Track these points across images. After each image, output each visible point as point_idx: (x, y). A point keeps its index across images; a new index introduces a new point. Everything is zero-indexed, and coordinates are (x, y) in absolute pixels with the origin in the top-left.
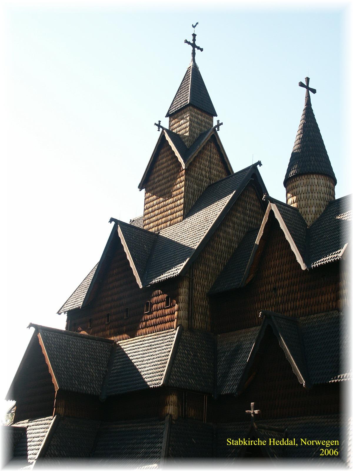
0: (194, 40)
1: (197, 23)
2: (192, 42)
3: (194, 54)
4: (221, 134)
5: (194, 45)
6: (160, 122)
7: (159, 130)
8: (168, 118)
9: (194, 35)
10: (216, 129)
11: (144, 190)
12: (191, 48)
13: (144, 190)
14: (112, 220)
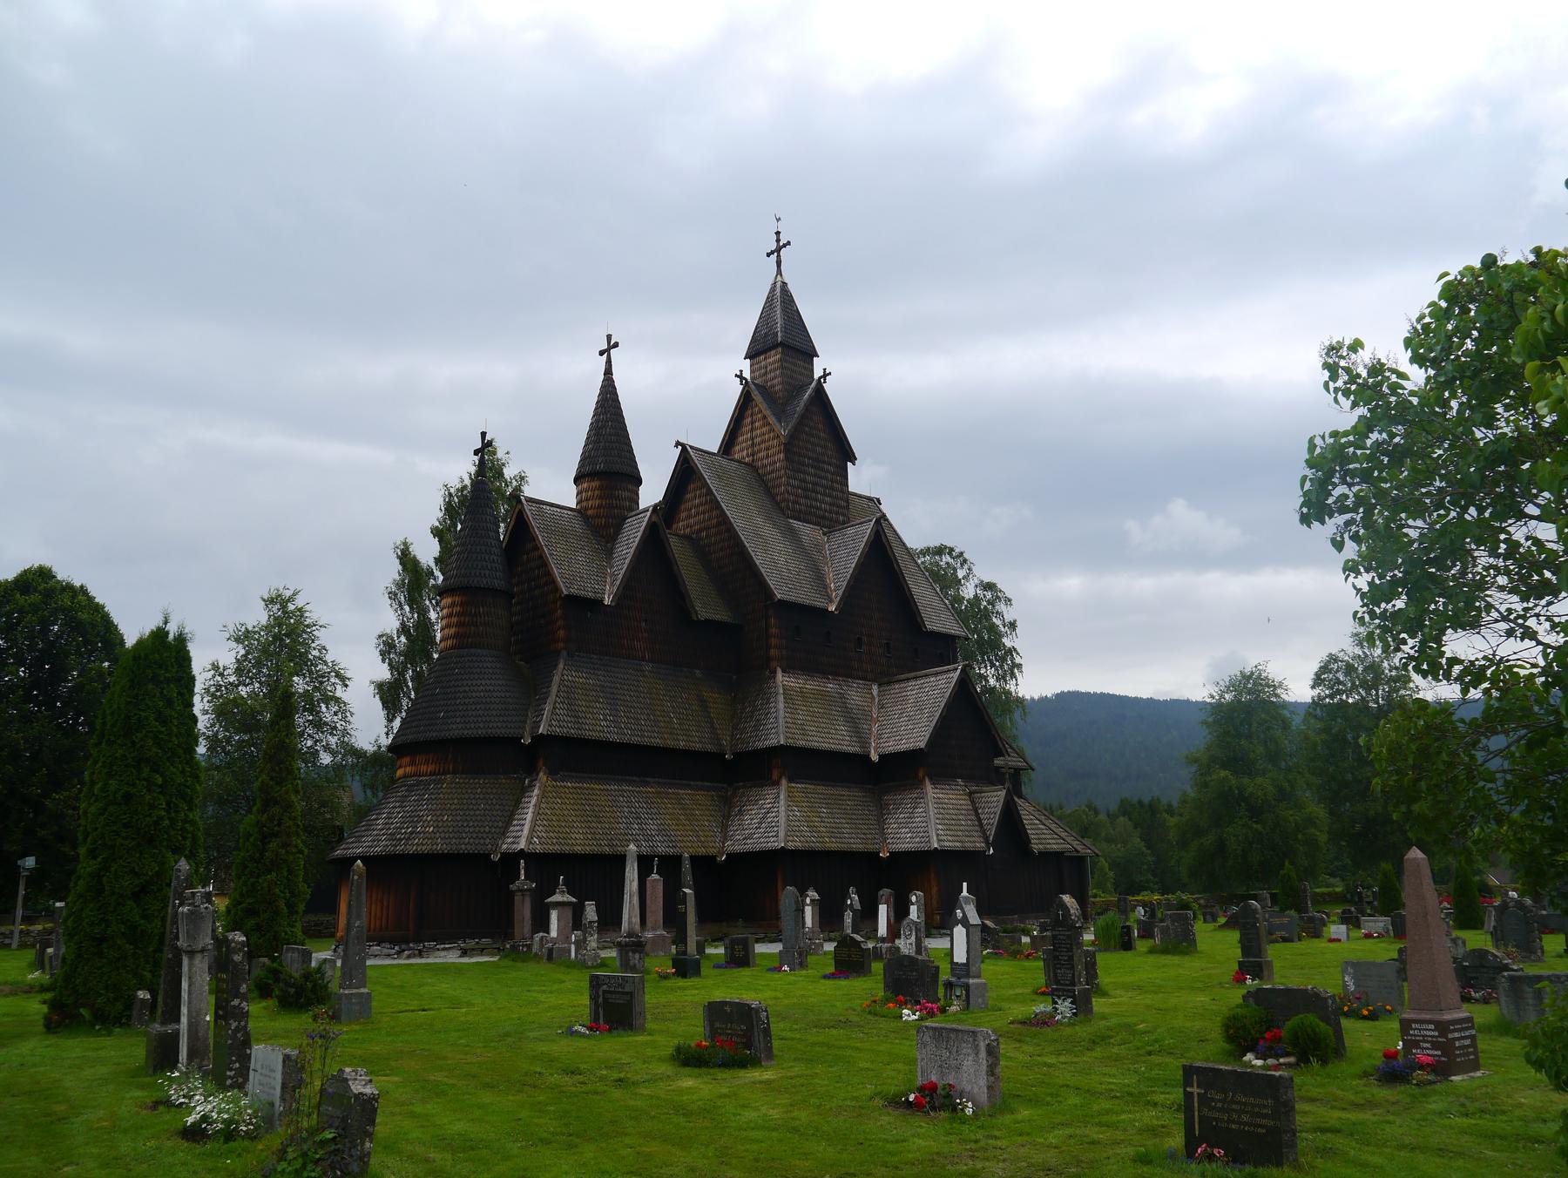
2: (776, 254)
4: (828, 387)
6: (741, 371)
7: (741, 384)
8: (748, 360)
10: (822, 380)
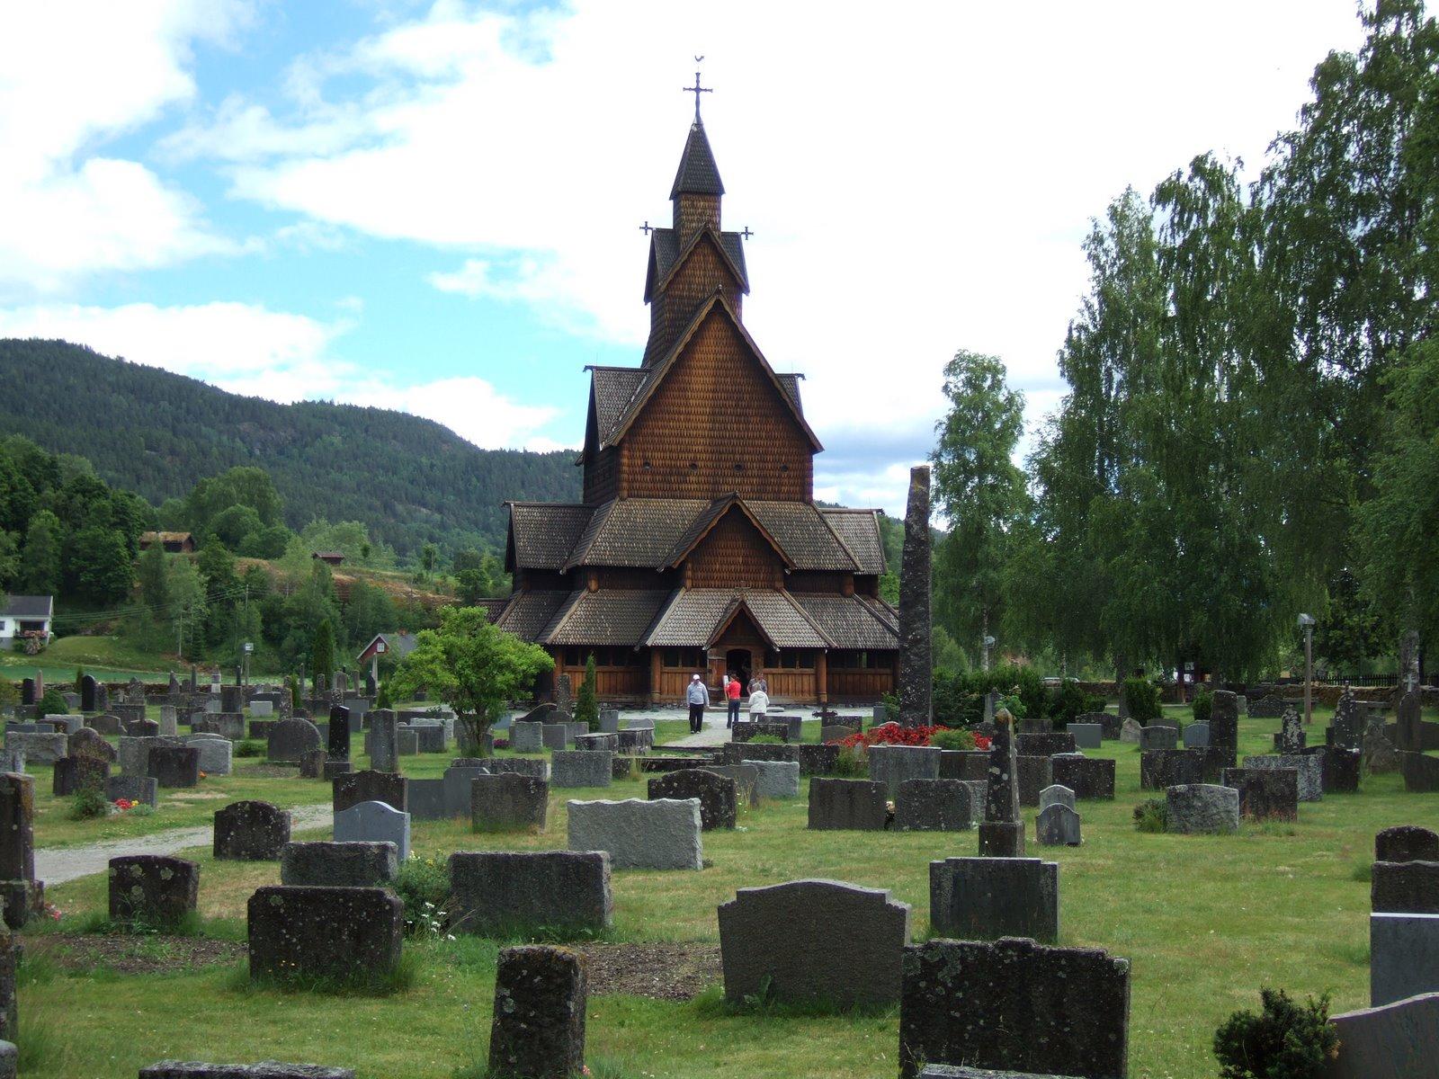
0: (698, 82)
1: (702, 57)
3: (698, 103)
5: (698, 90)
7: (646, 234)
9: (698, 74)
11: (649, 304)
12: (694, 93)
13: (649, 304)
14: (587, 368)
